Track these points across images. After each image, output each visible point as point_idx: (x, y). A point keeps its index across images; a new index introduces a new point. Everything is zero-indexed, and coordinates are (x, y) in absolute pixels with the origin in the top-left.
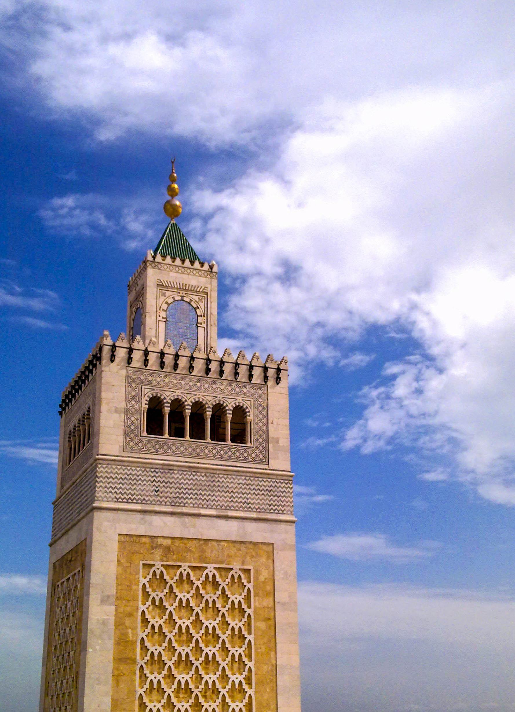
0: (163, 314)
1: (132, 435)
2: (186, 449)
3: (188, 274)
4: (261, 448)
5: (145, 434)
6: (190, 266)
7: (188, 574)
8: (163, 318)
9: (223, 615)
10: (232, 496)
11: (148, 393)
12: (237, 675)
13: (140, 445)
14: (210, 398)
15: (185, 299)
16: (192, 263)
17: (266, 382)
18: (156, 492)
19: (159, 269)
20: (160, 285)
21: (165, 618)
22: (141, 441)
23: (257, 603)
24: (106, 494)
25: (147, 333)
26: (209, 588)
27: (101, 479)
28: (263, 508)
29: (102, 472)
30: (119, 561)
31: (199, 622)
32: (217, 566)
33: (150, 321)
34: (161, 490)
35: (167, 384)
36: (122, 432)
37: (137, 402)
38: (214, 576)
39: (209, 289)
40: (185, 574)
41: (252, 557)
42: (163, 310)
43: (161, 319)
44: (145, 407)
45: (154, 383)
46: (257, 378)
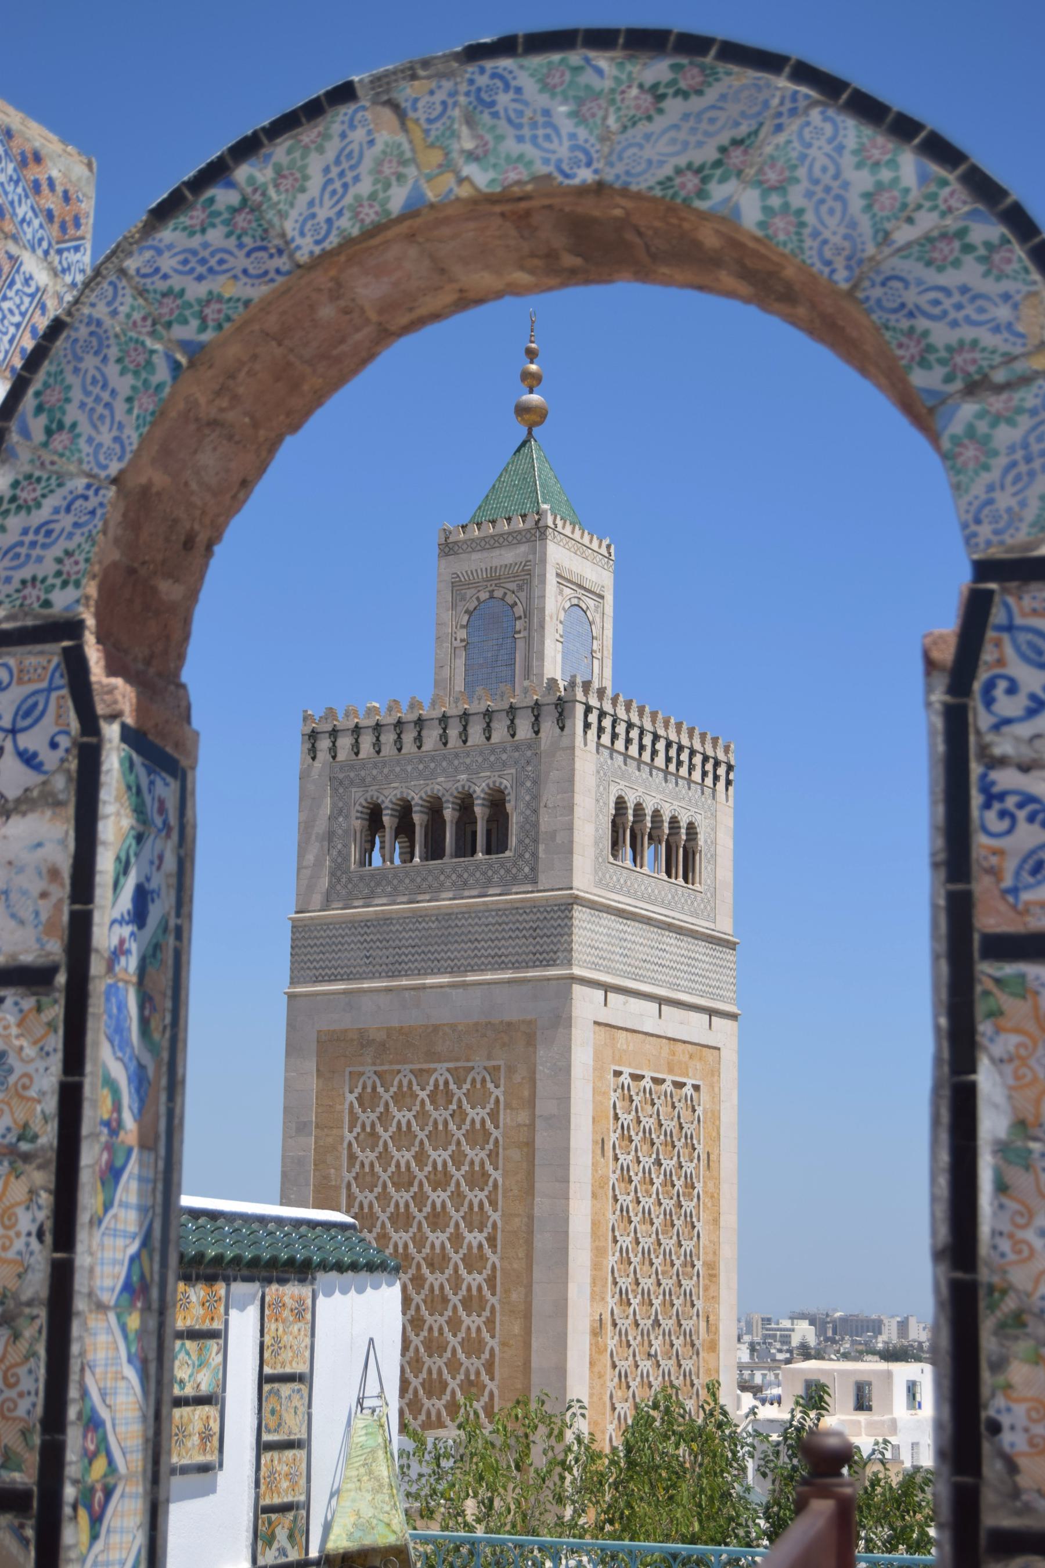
0: (462, 634)
7: (410, 1083)
8: (462, 641)
9: (458, 1143)
11: (359, 798)
17: (537, 733)
19: (456, 554)
21: (377, 1150)
23: (508, 1120)
26: (441, 1100)
28: (524, 961)
30: (318, 1070)
32: (451, 1065)
40: (405, 1083)
45: (368, 779)
46: (524, 730)
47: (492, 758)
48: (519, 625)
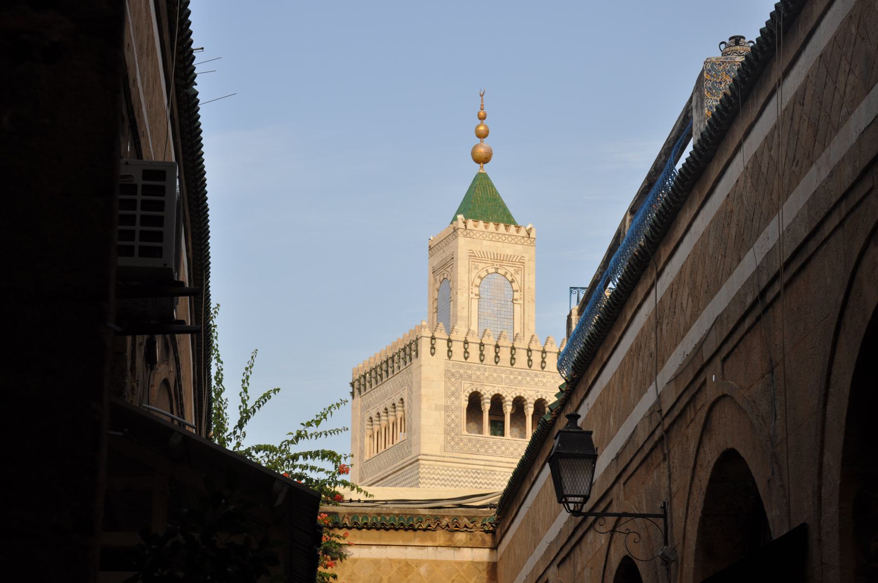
1: (453, 434)
2: (507, 449)
5: (465, 432)
6: (505, 232)
13: (461, 444)
14: (532, 393)
15: (499, 271)
16: (507, 227)
20: (472, 256)
22: (461, 440)
25: (459, 314)
33: (462, 298)
35: (487, 378)
36: (442, 431)
37: (457, 398)
39: (526, 259)
42: (476, 286)
44: (465, 404)
45: (473, 377)
48: (517, 295)
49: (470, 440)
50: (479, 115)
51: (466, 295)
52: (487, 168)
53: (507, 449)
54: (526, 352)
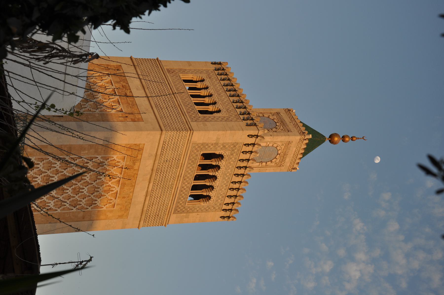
2: (189, 173)
3: (293, 157)
4: (184, 210)
10: (158, 197)
12: (53, 204)
13: (196, 151)
14: (217, 184)
15: (278, 156)
17: (223, 210)
18: (167, 161)
20: (289, 143)
22: (198, 151)
24: (169, 136)
27: (179, 134)
29: (183, 133)
31: (87, 184)
32: (118, 192)
34: (167, 163)
36: (205, 141)
37: (221, 149)
38: (112, 191)
39: (282, 168)
41: (121, 209)
43: (268, 143)
45: (232, 156)
47: (220, 197)
49: (197, 155)
50: (354, 137)
51: (270, 140)
52: (327, 142)
53: (189, 173)
54: (240, 180)
